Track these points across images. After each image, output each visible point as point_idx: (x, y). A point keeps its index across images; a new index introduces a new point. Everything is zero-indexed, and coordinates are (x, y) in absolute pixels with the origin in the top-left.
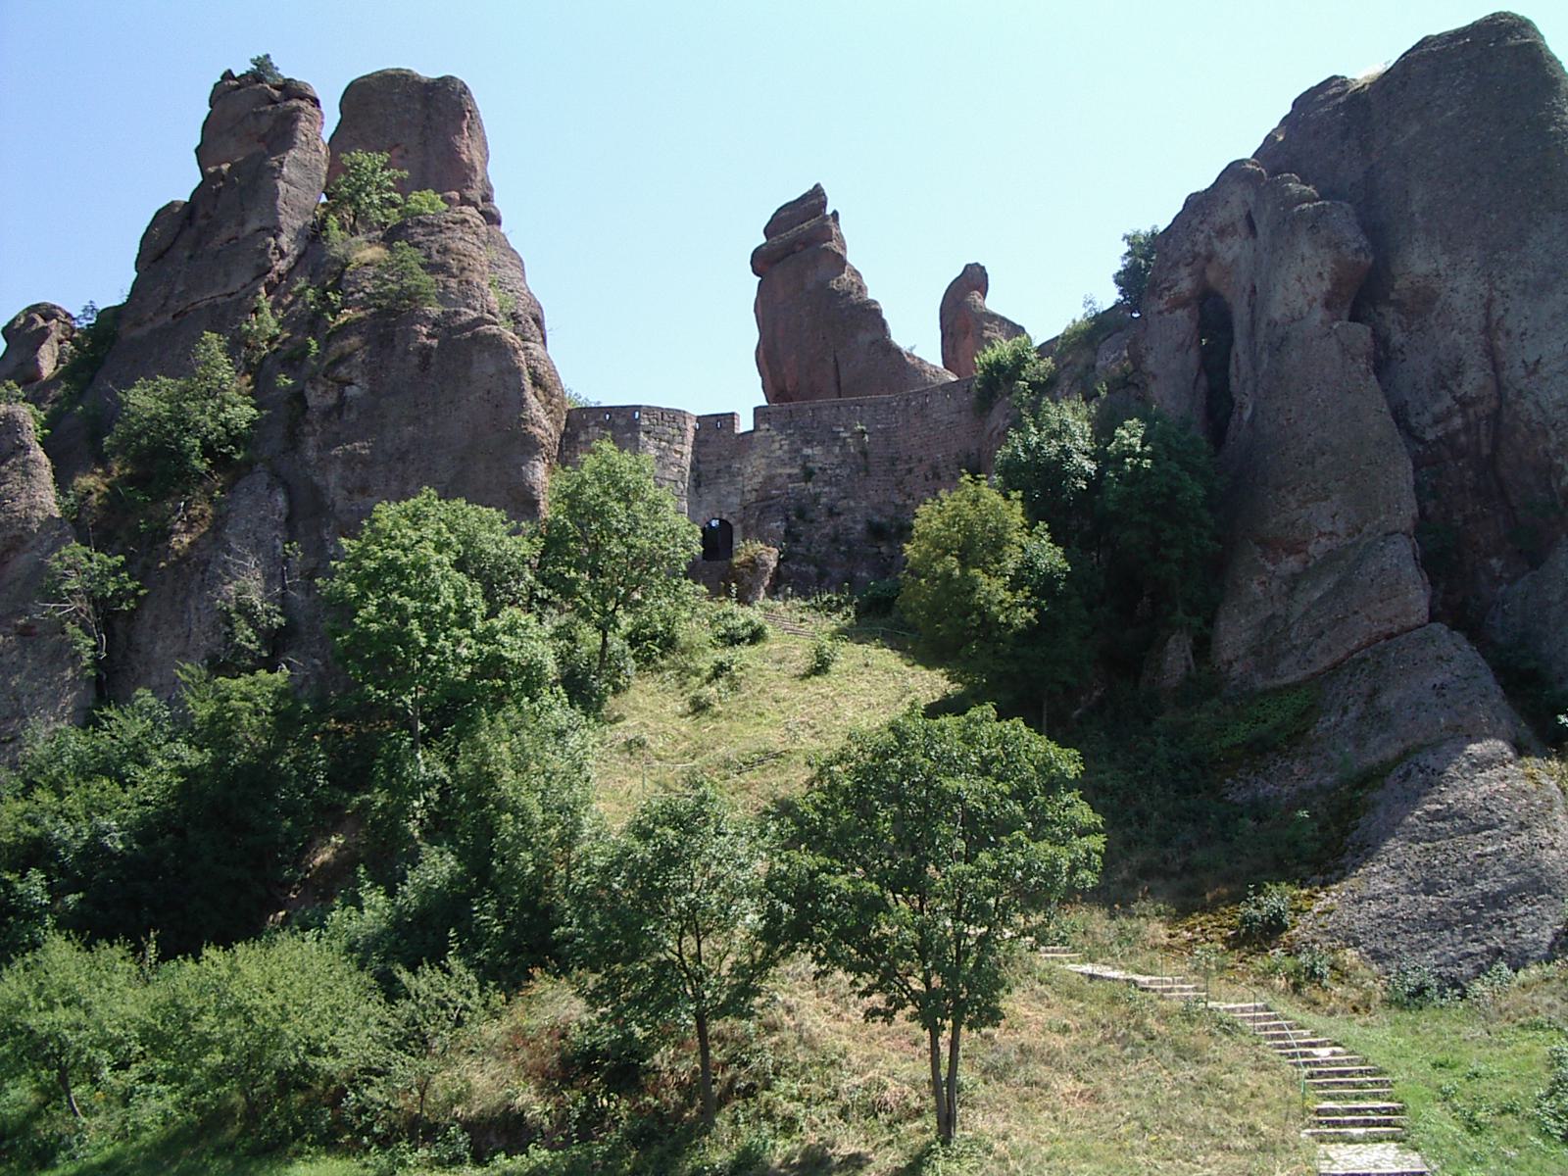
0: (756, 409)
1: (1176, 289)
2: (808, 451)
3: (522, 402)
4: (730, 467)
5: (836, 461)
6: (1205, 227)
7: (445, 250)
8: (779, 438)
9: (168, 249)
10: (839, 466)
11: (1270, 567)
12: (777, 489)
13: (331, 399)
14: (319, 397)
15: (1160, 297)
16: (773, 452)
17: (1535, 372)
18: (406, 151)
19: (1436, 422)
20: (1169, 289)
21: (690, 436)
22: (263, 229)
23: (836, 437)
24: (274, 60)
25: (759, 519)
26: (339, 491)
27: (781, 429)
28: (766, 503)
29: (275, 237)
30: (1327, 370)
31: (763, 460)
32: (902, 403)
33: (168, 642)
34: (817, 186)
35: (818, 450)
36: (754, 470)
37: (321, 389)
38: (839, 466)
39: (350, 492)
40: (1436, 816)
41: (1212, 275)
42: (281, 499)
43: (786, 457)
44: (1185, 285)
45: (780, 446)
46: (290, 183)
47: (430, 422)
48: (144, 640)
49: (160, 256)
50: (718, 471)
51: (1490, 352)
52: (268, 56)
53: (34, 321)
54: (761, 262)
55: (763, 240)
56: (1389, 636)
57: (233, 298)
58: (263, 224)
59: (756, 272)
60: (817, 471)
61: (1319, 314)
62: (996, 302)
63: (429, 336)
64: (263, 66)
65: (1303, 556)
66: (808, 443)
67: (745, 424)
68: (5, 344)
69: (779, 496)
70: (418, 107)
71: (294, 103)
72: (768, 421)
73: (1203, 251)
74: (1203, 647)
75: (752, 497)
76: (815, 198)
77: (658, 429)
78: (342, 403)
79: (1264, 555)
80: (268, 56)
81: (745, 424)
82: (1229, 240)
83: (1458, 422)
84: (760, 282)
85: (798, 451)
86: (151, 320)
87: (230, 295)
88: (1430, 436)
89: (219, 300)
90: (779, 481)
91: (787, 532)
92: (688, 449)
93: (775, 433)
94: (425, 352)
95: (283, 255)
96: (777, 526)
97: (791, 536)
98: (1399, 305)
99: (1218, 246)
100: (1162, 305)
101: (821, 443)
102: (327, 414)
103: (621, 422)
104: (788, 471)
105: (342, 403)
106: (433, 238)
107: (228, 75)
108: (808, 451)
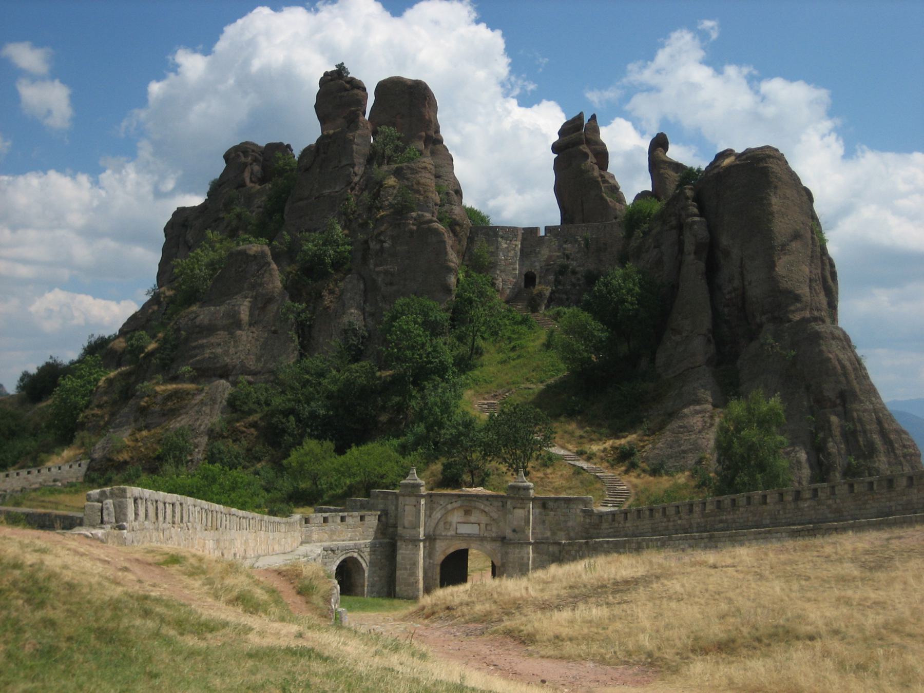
0: (546, 227)
2: (565, 246)
3: (446, 253)
5: (577, 250)
7: (418, 183)
13: (378, 247)
14: (373, 245)
17: (750, 284)
21: (520, 237)
22: (347, 165)
23: (576, 241)
24: (345, 65)
29: (353, 168)
34: (581, 114)
36: (545, 252)
40: (681, 427)
42: (362, 286)
44: (674, 223)
46: (358, 145)
51: (742, 274)
52: (343, 63)
53: (239, 156)
56: (692, 368)
59: (554, 152)
61: (692, 256)
63: (413, 224)
64: (341, 71)
66: (565, 242)
67: (542, 233)
68: (225, 165)
71: (356, 91)
74: (653, 360)
75: (543, 264)
76: (580, 117)
77: (506, 236)
80: (343, 63)
81: (542, 233)
83: (733, 294)
87: (337, 192)
88: (728, 297)
91: (556, 280)
92: (519, 243)
94: (411, 232)
95: (356, 175)
96: (551, 278)
97: (557, 282)
101: (571, 243)
103: (491, 233)
104: (558, 254)
105: (382, 250)
106: (413, 176)
107: (326, 74)
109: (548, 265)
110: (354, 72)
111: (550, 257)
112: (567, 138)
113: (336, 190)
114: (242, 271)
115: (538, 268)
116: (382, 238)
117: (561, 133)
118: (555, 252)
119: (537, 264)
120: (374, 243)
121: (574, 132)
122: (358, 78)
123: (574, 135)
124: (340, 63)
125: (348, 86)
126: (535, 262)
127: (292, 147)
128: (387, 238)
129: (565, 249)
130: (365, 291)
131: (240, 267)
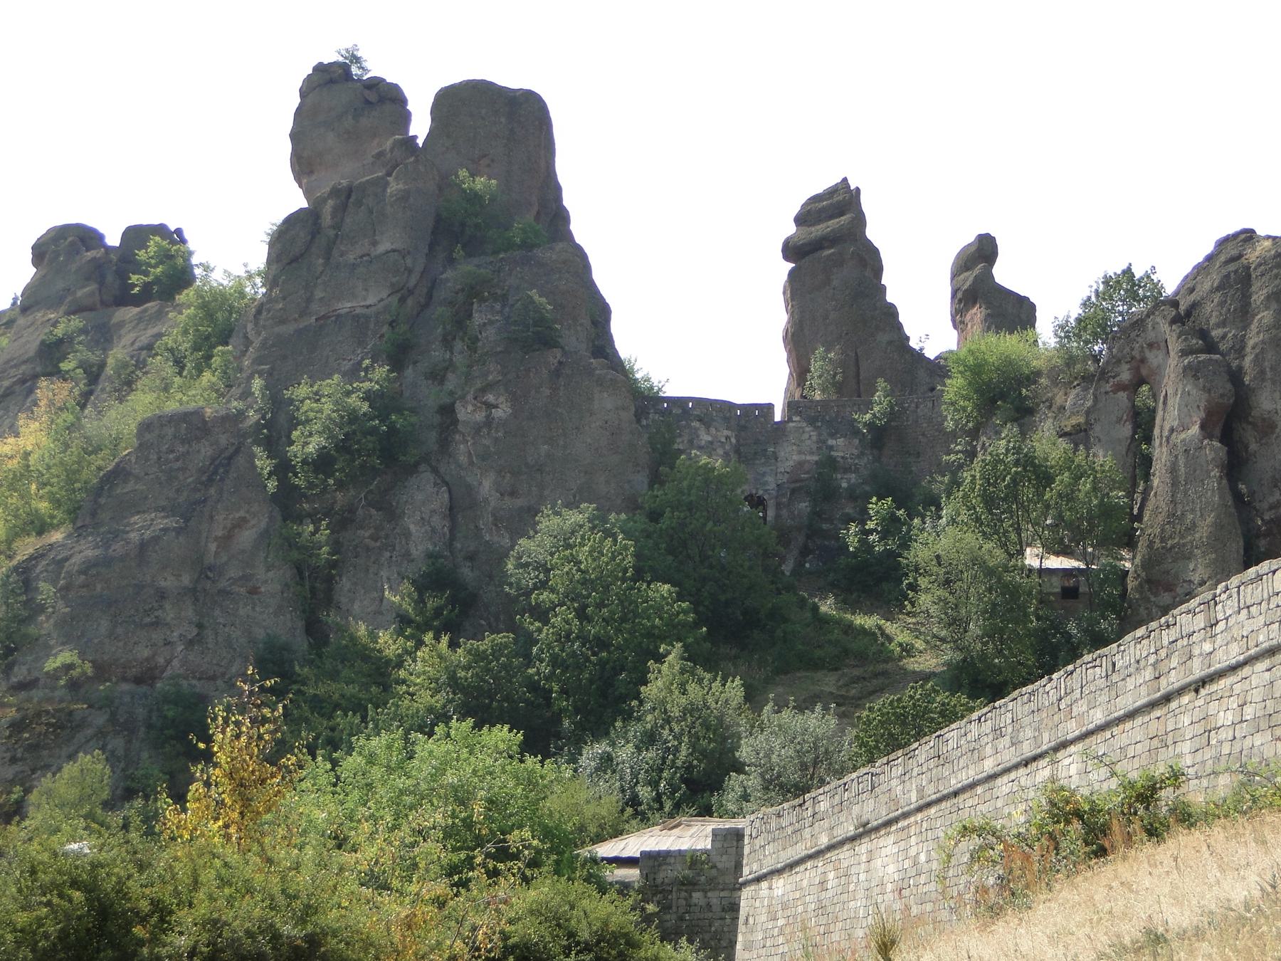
1: (1118, 378)
2: (831, 442)
4: (766, 450)
5: (855, 452)
6: (1139, 339)
8: (807, 429)
9: (302, 255)
10: (858, 457)
11: (1153, 599)
12: (807, 473)
13: (480, 416)
14: (467, 413)
15: (1107, 382)
16: (802, 441)
18: (493, 161)
19: (1271, 508)
20: (1114, 377)
23: (857, 432)
25: (790, 499)
26: (493, 492)
27: (812, 421)
28: (798, 485)
30: (1198, 472)
31: (794, 447)
32: (913, 405)
33: (365, 603)
34: (845, 180)
35: (841, 441)
37: (470, 408)
38: (858, 457)
39: (502, 495)
41: (1144, 372)
43: (814, 447)
44: (1125, 376)
45: (810, 435)
47: (561, 443)
48: (344, 600)
49: (295, 260)
50: (756, 453)
54: (791, 250)
55: (791, 229)
57: (373, 309)
58: (393, 247)
60: (839, 459)
62: (1005, 274)
65: (1173, 593)
66: (833, 436)
69: (807, 479)
70: (503, 120)
72: (800, 413)
73: (1138, 356)
75: (785, 478)
78: (489, 422)
79: (1150, 589)
82: (1155, 351)
84: (792, 274)
85: (824, 442)
86: (295, 320)
87: (368, 307)
89: (358, 311)
90: (807, 467)
93: (805, 424)
98: (1254, 425)
99: (1147, 352)
100: (1108, 387)
102: (477, 429)
107: (320, 69)
108: (831, 442)
109: (796, 481)
110: (378, 66)
111: (801, 464)
112: (819, 230)
113: (368, 303)
114: (177, 459)
115: (772, 486)
116: (490, 398)
117: (800, 220)
118: (812, 453)
119: (770, 479)
120: (470, 408)
121: (831, 217)
122: (390, 79)
123: (833, 224)
124: (349, 45)
125: (372, 97)
126: (764, 474)
127: (187, 235)
128: (502, 399)
129: (831, 448)
130: (451, 509)
131: (172, 451)
